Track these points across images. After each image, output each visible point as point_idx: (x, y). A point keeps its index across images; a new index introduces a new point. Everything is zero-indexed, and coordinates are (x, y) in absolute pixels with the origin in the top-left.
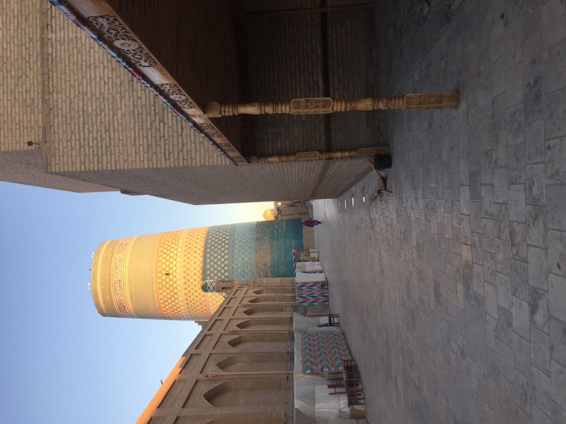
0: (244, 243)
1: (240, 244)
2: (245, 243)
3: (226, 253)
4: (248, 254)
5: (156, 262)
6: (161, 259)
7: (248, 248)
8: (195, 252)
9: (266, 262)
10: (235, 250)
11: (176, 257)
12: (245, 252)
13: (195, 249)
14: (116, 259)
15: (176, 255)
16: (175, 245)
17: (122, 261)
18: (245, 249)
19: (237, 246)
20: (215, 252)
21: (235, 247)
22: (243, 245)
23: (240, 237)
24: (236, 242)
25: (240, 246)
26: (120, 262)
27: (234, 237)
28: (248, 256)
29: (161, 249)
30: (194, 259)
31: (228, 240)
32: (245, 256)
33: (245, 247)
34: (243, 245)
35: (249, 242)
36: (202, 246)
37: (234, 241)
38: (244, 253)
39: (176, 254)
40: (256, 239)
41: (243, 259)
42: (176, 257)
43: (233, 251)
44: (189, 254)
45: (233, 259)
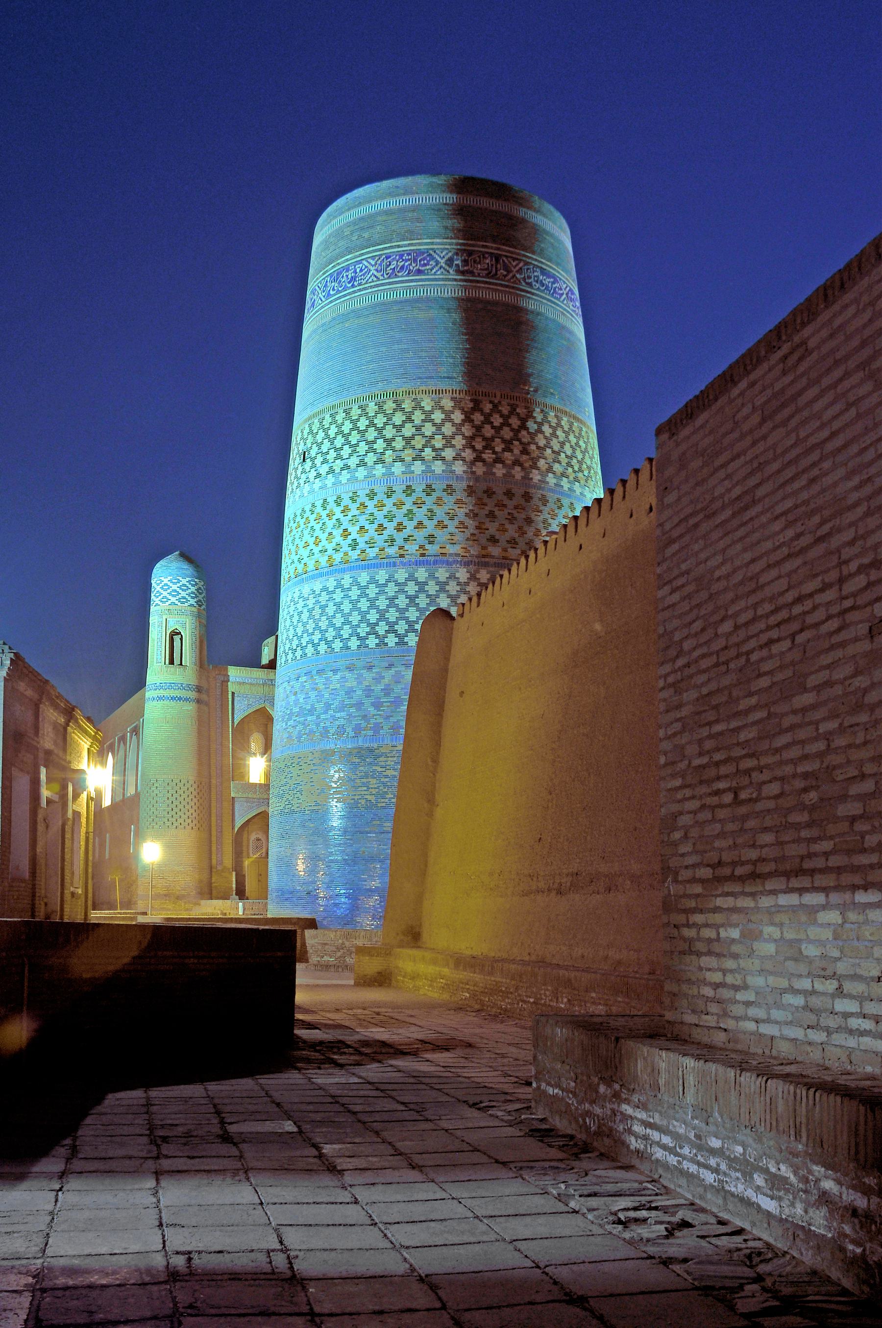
0: (359, 705)
1: (359, 692)
2: (359, 709)
3: (333, 646)
4: (322, 725)
5: (333, 407)
6: (340, 418)
7: (342, 722)
8: (346, 533)
9: (301, 791)
10: (338, 677)
11: (337, 470)
12: (331, 712)
13: (354, 530)
14: (360, 262)
15: (342, 469)
16: (383, 454)
17: (353, 286)
18: (338, 715)
19: (351, 683)
20: (338, 605)
21: (348, 675)
22: (352, 706)
23: (387, 691)
24: (368, 676)
25: (350, 692)
26: (349, 283)
27: (391, 666)
28: (318, 725)
29: (372, 408)
30: (326, 534)
31: (382, 643)
32: (318, 717)
33: (343, 714)
34: (352, 706)
35: (364, 724)
36: (363, 551)
37: (370, 668)
38: (326, 712)
39: (346, 467)
40: (371, 750)
41: (311, 711)
42: (337, 470)
43: (335, 671)
44: (343, 512)
45: (314, 672)
